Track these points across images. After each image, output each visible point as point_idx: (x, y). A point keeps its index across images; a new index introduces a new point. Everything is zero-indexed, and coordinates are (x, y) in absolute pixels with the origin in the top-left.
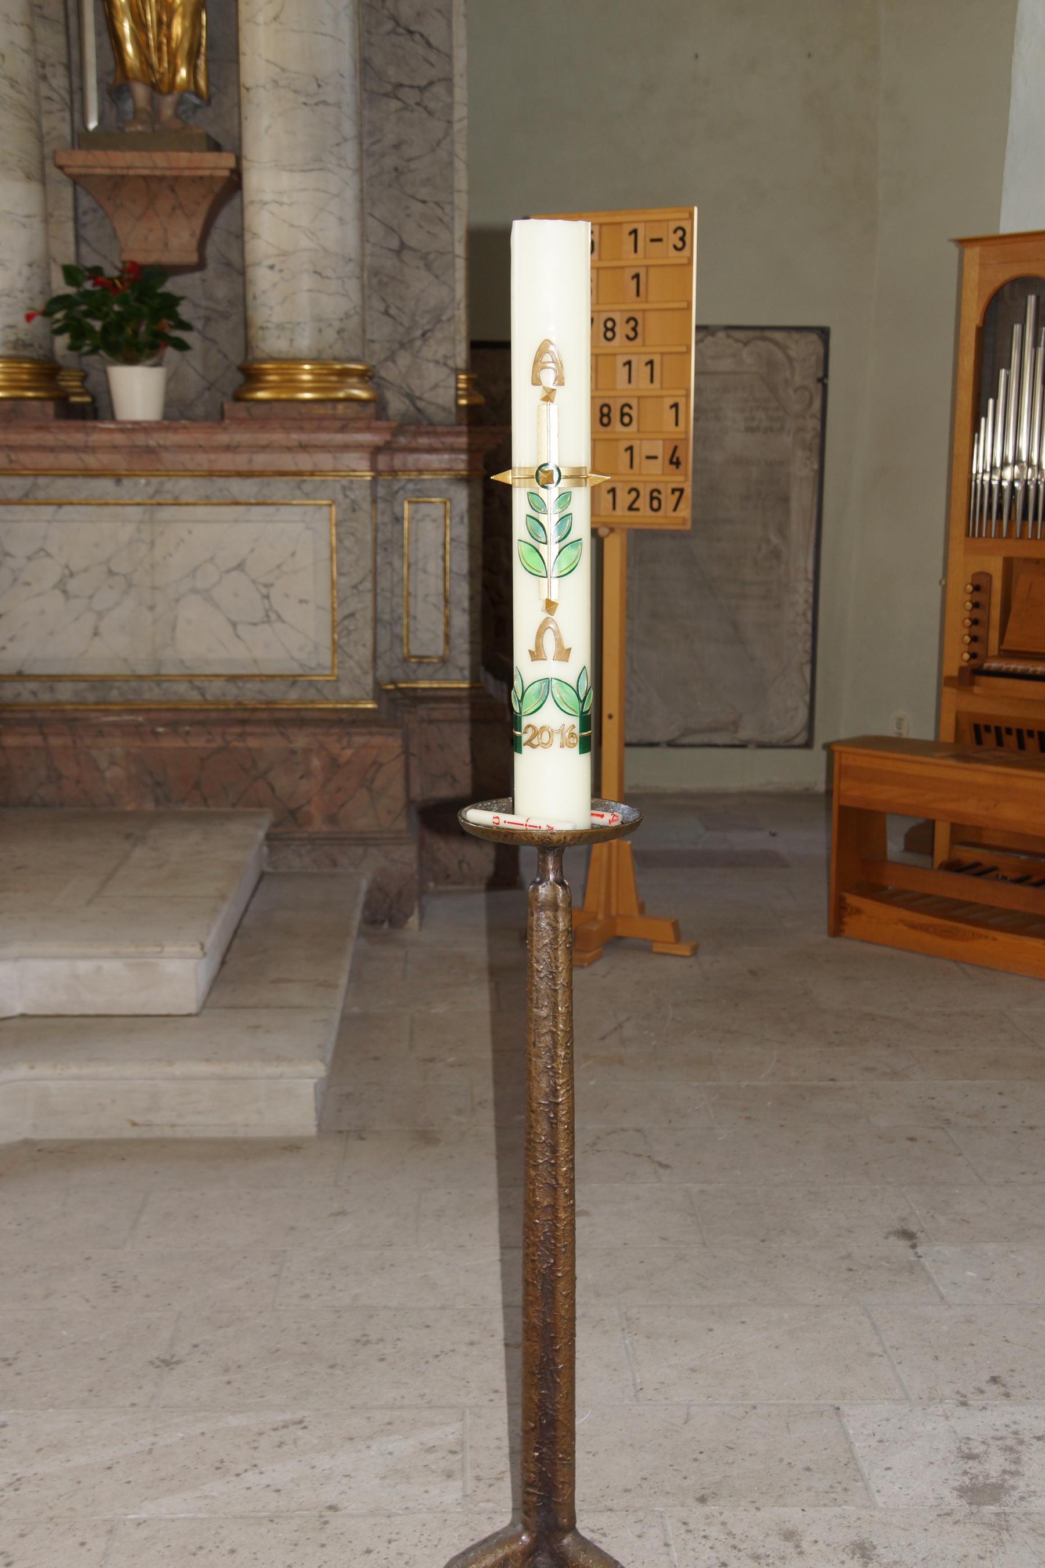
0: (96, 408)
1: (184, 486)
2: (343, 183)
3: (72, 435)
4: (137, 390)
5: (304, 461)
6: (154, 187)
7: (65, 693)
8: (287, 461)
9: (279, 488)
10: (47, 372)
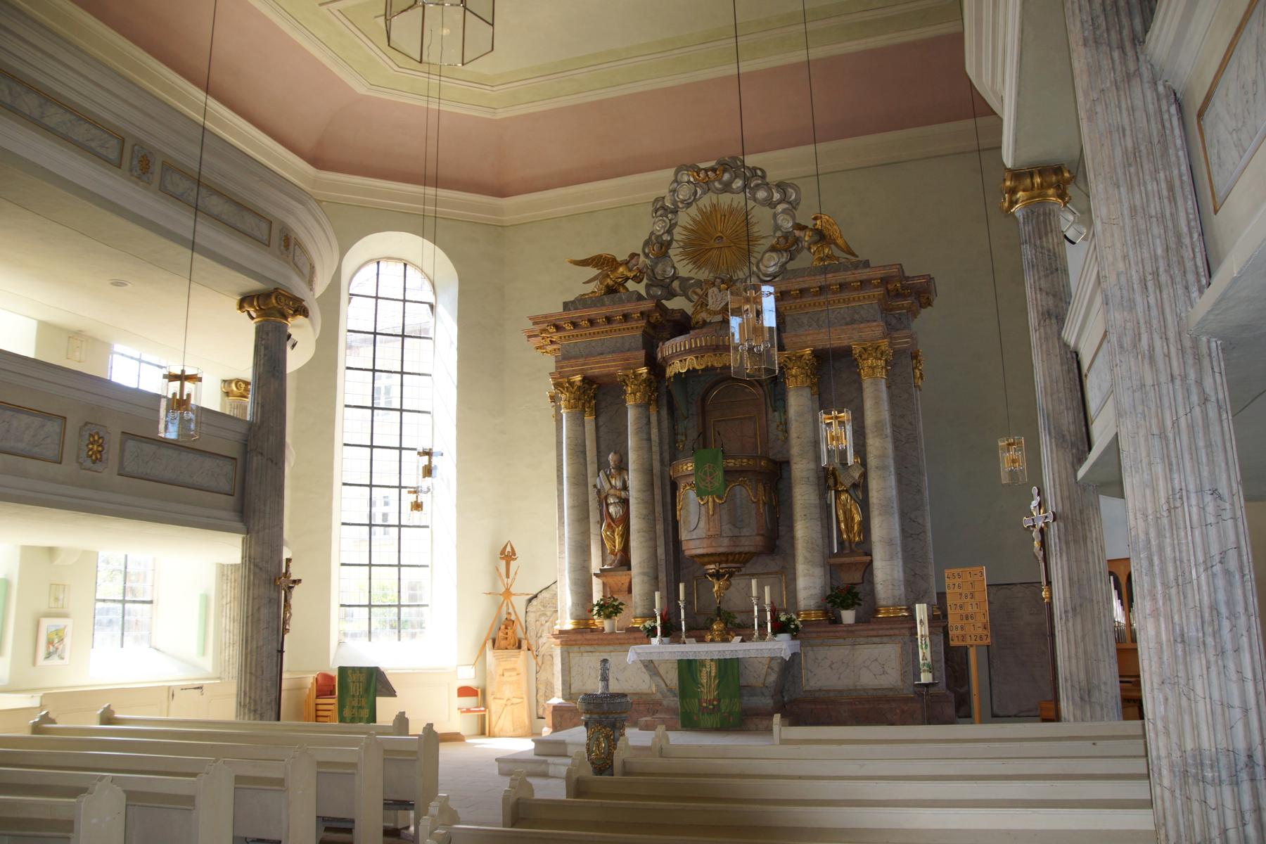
0: (837, 621)
1: (862, 640)
2: (899, 563)
3: (834, 628)
4: (848, 616)
5: (892, 632)
6: (850, 566)
7: (832, 694)
8: (887, 633)
9: (885, 640)
10: (826, 612)
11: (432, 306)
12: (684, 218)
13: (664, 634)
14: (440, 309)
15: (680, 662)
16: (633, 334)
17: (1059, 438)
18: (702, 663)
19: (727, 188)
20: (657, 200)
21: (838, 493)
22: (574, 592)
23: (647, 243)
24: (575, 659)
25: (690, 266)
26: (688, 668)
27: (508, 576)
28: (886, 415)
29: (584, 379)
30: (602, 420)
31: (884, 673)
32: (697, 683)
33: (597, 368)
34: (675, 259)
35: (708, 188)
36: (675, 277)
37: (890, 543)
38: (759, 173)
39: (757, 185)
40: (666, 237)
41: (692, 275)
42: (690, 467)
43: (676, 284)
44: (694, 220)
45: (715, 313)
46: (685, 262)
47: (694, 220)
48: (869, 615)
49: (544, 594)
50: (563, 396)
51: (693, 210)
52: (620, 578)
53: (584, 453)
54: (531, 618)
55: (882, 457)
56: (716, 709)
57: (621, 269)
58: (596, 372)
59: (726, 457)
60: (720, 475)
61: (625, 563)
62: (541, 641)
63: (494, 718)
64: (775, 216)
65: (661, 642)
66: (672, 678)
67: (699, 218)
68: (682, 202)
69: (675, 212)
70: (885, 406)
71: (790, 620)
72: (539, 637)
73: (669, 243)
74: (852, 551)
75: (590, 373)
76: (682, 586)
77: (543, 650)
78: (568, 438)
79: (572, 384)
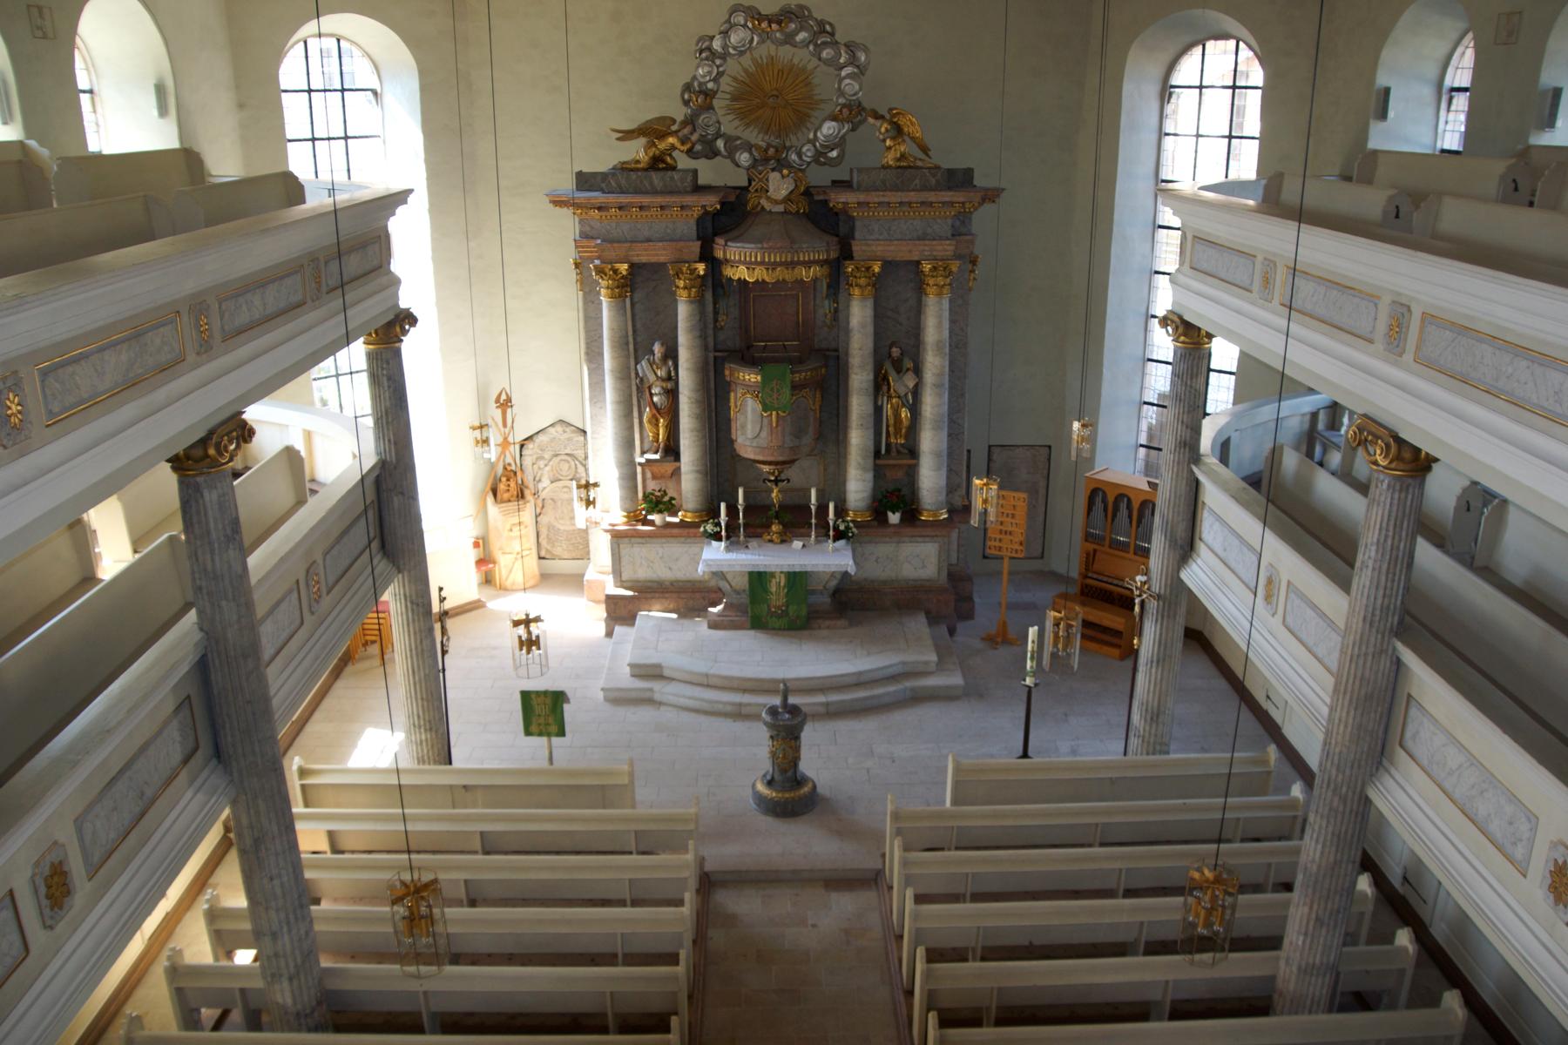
4: (894, 518)
11: (375, 93)
12: (732, 67)
13: (728, 537)
14: (388, 97)
15: (751, 574)
16: (686, 225)
17: (1172, 541)
18: (772, 575)
19: (789, 40)
20: (701, 39)
21: (890, 397)
22: (622, 487)
23: (688, 87)
24: (626, 549)
25: (737, 123)
26: (758, 579)
27: (505, 425)
28: (946, 333)
29: (632, 266)
30: (638, 296)
31: (924, 567)
32: (766, 591)
33: (644, 255)
34: (720, 112)
35: (766, 37)
36: (718, 135)
37: (938, 455)
38: (828, 28)
39: (824, 43)
40: (710, 85)
41: (738, 133)
42: (751, 377)
43: (720, 144)
44: (746, 71)
45: (776, 202)
46: (730, 117)
47: (746, 71)
48: (911, 514)
49: (541, 438)
50: (604, 283)
51: (746, 60)
52: (669, 467)
53: (627, 344)
54: (528, 461)
55: (940, 375)
56: (785, 614)
57: (671, 140)
58: (644, 259)
59: (792, 372)
60: (787, 391)
61: (672, 451)
62: (541, 486)
63: (504, 572)
64: (841, 80)
65: (728, 549)
66: (742, 583)
67: (752, 69)
68: (735, 48)
69: (724, 56)
70: (946, 325)
71: (848, 528)
72: (538, 481)
73: (715, 93)
74: (898, 452)
75: (636, 260)
76: (741, 491)
77: (543, 495)
78: (611, 329)
79: (615, 271)
